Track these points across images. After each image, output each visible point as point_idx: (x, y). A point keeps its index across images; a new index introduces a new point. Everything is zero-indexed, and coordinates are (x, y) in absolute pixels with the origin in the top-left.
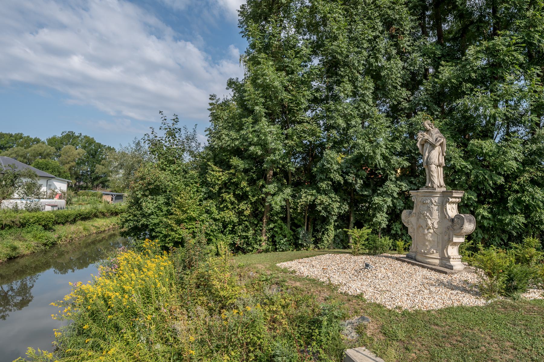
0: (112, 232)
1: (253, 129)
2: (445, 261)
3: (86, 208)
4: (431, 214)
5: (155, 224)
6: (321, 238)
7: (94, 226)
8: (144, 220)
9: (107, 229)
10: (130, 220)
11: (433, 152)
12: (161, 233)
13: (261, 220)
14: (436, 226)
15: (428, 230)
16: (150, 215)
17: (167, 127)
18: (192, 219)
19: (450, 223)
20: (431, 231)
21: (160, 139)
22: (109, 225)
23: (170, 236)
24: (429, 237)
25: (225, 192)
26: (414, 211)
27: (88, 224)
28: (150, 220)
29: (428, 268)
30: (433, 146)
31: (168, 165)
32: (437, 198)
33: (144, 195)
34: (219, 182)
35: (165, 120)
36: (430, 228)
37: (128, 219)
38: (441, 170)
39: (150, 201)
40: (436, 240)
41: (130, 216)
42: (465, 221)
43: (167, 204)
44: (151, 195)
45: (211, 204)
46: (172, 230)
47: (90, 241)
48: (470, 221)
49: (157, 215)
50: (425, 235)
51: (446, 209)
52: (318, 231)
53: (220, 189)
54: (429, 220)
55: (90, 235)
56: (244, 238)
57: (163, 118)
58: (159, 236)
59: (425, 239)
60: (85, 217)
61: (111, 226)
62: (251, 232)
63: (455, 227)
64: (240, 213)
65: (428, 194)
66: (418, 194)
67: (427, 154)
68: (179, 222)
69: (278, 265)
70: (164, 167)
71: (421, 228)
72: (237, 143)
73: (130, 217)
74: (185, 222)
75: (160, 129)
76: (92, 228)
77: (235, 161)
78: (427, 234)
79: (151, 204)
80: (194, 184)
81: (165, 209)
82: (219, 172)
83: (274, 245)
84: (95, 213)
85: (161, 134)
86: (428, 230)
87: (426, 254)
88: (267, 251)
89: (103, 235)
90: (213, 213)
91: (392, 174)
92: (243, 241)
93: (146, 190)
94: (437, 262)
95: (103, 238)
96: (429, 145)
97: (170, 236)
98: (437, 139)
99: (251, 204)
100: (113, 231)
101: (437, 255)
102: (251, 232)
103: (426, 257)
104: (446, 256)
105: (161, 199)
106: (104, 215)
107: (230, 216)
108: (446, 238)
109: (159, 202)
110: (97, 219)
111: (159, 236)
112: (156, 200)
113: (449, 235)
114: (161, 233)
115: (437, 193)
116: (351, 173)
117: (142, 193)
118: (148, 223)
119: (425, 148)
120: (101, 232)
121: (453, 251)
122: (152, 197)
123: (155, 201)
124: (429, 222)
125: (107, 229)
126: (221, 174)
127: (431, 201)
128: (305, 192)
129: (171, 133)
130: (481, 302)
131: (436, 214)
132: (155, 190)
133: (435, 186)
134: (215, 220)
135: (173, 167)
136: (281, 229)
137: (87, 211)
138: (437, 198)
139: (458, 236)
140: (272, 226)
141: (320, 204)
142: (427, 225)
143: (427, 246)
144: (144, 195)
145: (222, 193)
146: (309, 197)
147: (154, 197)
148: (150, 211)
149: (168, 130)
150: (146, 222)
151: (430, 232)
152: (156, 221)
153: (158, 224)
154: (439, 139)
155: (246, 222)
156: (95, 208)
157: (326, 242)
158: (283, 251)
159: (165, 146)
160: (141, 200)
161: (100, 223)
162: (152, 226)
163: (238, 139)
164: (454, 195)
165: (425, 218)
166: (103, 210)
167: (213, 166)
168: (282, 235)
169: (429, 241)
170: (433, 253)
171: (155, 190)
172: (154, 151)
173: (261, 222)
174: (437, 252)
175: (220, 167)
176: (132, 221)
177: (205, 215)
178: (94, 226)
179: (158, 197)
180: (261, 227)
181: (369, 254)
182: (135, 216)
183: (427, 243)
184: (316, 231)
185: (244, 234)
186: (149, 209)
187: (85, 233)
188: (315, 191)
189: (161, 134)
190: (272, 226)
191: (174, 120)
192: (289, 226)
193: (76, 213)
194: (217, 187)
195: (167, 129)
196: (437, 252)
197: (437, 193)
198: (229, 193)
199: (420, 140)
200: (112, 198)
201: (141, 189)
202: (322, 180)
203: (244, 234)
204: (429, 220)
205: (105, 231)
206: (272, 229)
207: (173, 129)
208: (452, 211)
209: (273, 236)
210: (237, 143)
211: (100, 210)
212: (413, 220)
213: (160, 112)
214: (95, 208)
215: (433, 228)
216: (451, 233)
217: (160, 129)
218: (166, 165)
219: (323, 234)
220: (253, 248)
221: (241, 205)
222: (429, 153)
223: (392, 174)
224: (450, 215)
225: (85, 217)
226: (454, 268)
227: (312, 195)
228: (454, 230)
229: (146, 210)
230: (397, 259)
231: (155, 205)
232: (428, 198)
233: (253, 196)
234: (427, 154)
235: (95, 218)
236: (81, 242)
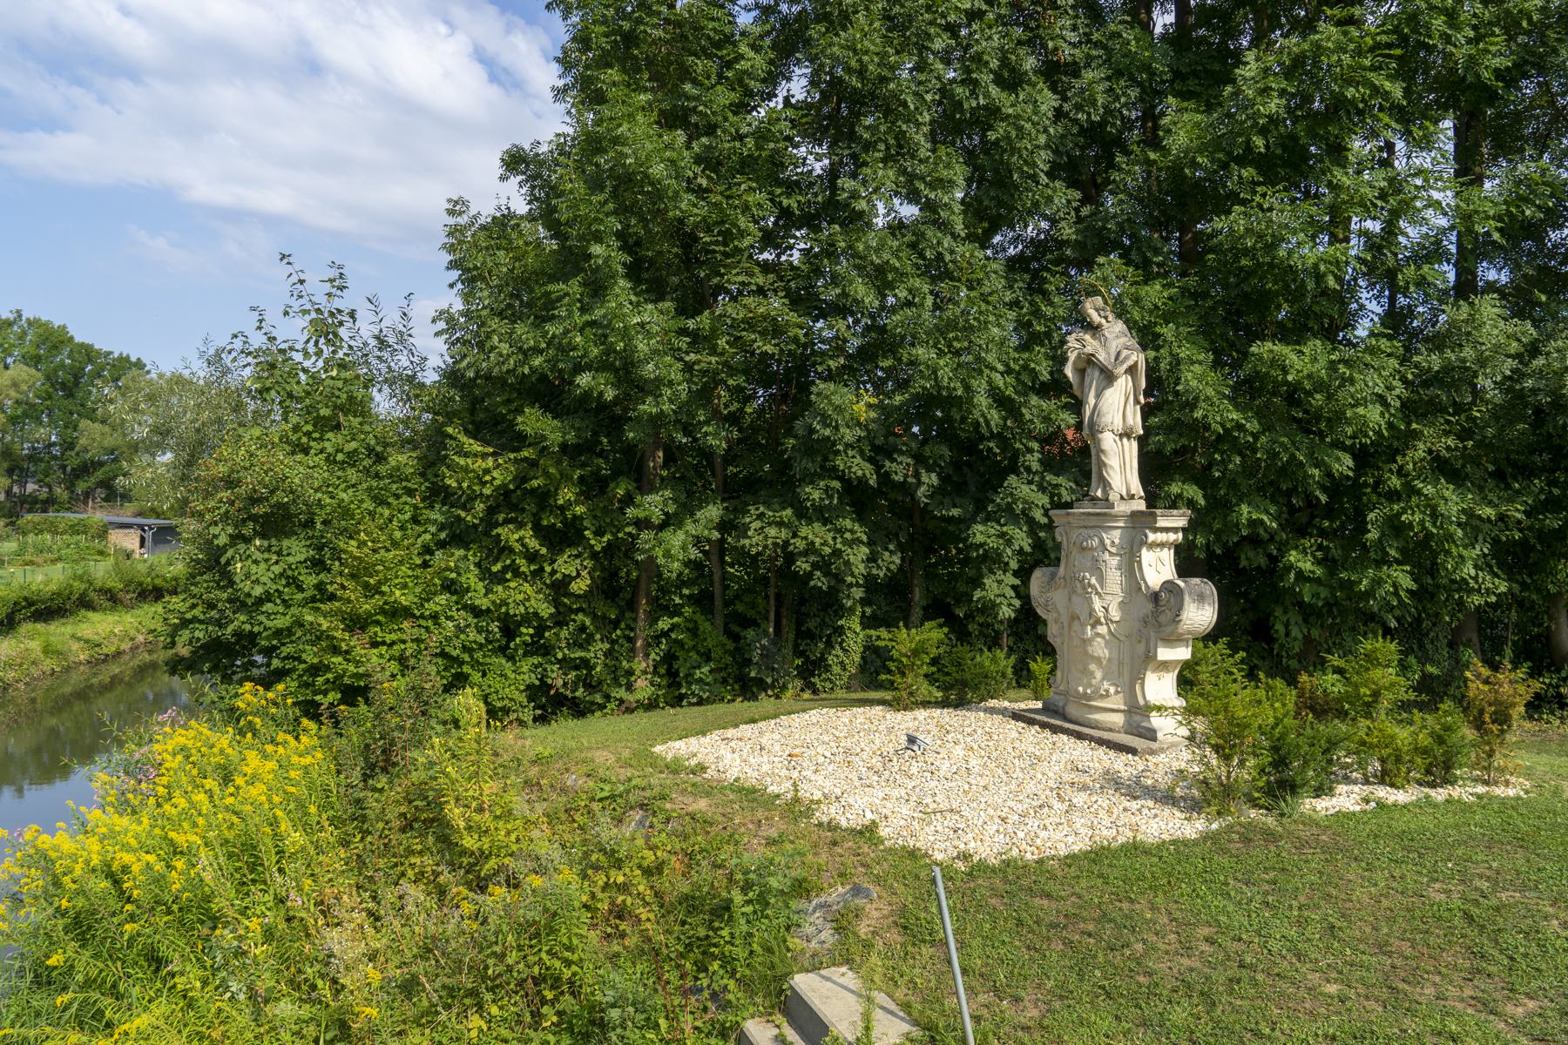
0: (147, 658)
1: (587, 317)
2: (1137, 718)
3: (47, 578)
5: (278, 633)
6: (823, 659)
7: (79, 639)
8: (243, 618)
9: (126, 646)
10: (195, 620)
11: (1109, 393)
12: (299, 659)
13: (632, 605)
14: (1115, 614)
15: (1093, 627)
16: (260, 601)
17: (308, 307)
18: (397, 613)
19: (1150, 606)
20: (1102, 630)
21: (283, 346)
22: (132, 633)
23: (328, 668)
24: (1100, 649)
25: (507, 522)
26: (1062, 570)
27: (59, 631)
28: (262, 618)
29: (1091, 739)
30: (1109, 377)
31: (316, 435)
32: (1117, 533)
33: (236, 538)
34: (487, 491)
35: (302, 282)
36: (1098, 622)
37: (188, 616)
38: (1132, 448)
39: (258, 556)
41: (194, 606)
42: (1187, 598)
43: (318, 565)
44: (263, 536)
45: (462, 563)
46: (335, 650)
47: (67, 689)
48: (1201, 598)
49: (284, 601)
50: (1086, 642)
51: (1140, 562)
52: (810, 636)
53: (491, 511)
54: (1095, 599)
55: (67, 670)
56: (577, 668)
57: (295, 278)
58: (294, 669)
59: (1086, 652)
60: (48, 609)
61: (141, 638)
62: (600, 647)
63: (1162, 618)
64: (560, 587)
65: (1093, 521)
66: (1071, 519)
68: (357, 623)
69: (658, 749)
70: (304, 440)
72: (537, 361)
73: (196, 612)
74: (378, 623)
75: (286, 313)
76: (75, 646)
77: (532, 420)
78: (1091, 640)
79: (263, 566)
80: (405, 498)
81: (310, 580)
82: (484, 456)
83: (674, 689)
84: (83, 595)
85: (294, 331)
86: (1093, 627)
87: (1089, 698)
88: (651, 705)
89: (115, 669)
90: (468, 590)
91: (1030, 451)
92: (572, 675)
93: (244, 521)
94: (1118, 719)
95: (115, 681)
96: (1097, 373)
97: (328, 668)
98: (1118, 354)
99: (594, 556)
100: (150, 652)
101: (1117, 702)
102: (600, 647)
103: (1090, 707)
104: (1141, 702)
105: (297, 549)
106: (112, 599)
107: (527, 597)
108: (1141, 648)
109: (290, 559)
110: (90, 614)
111: (294, 669)
112: (279, 553)
113: (1148, 642)
114: (299, 659)
115: (1115, 517)
116: (902, 453)
117: (230, 530)
118: (256, 629)
119: (1087, 379)
120: (106, 659)
121: (1160, 688)
122: (266, 543)
123: (275, 557)
124: (1097, 605)
125: (126, 646)
126: (490, 462)
127: (1102, 541)
128: (761, 516)
129: (326, 328)
130: (1191, 828)
131: (1115, 579)
132: (277, 521)
133: (1113, 497)
134: (477, 612)
135: (333, 440)
136: (694, 631)
137: (53, 587)
138: (1117, 533)
139: (1173, 640)
140: (664, 624)
141: (806, 553)
142: (1091, 612)
144: (236, 538)
145: (497, 525)
146: (772, 532)
147: (274, 542)
148: (258, 591)
149: (314, 315)
150: (248, 627)
151: (1098, 635)
152: (281, 622)
153: (289, 631)
154: (1125, 353)
155: (580, 616)
156: (80, 578)
157: (836, 669)
158: (700, 702)
159: (305, 371)
160: (229, 554)
161: (102, 626)
162: (267, 638)
163: (541, 352)
164: (1161, 523)
166: (110, 584)
167: (463, 438)
168: (698, 653)
170: (1107, 695)
171: (277, 521)
172: (268, 390)
173: (628, 615)
175: (487, 443)
176: (201, 622)
177: (442, 599)
178: (79, 639)
179: (286, 543)
180: (632, 629)
181: (943, 704)
182: (211, 606)
184: (804, 635)
185: (579, 654)
186: (257, 582)
187: (48, 664)
188: (789, 512)
189: (294, 331)
190: (664, 624)
191: (331, 281)
192: (719, 621)
193: (13, 596)
194: (480, 507)
195: (308, 312)
197: (1115, 517)
198: (521, 526)
199: (1072, 356)
200: (143, 540)
201: (226, 517)
202: (811, 479)
203: (579, 654)
204: (1095, 599)
205: (119, 654)
206: (665, 634)
207: (332, 314)
208: (1158, 567)
209: (669, 658)
210: (537, 361)
211: (98, 584)
212: (1059, 597)
213: (283, 257)
214: (80, 578)
215: (1109, 620)
217: (286, 313)
218: (308, 434)
219: (829, 645)
220: (608, 697)
221: (560, 561)
223: (1030, 451)
224: (1150, 584)
225: (48, 609)
226: (1160, 735)
227: (780, 524)
229: (246, 586)
230: (1016, 716)
231: (277, 569)
232: (1091, 532)
233: (599, 533)
234: (1092, 400)
235: (83, 611)
236: (38, 694)
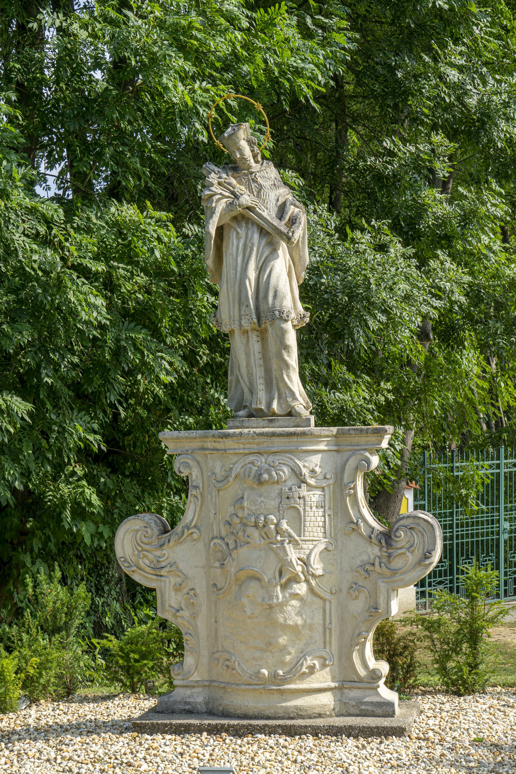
2: (354, 694)
4: (299, 522)
14: (318, 567)
15: (284, 587)
19: (373, 551)
20: (301, 589)
24: (292, 614)
36: (295, 579)
40: (318, 619)
54: (289, 548)
59: (274, 624)
63: (397, 563)
65: (279, 443)
67: (252, 274)
71: (254, 584)
78: (282, 605)
86: (284, 587)
87: (285, 680)
94: (327, 700)
104: (362, 672)
113: (374, 595)
124: (293, 555)
127: (297, 474)
138: (316, 459)
143: (284, 650)
151: (295, 596)
165: (273, 542)
169: (295, 630)
174: (324, 666)
183: (283, 640)
196: (324, 666)
204: (289, 548)
216: (382, 586)
222: (261, 270)
228: (395, 572)
234: (252, 274)
